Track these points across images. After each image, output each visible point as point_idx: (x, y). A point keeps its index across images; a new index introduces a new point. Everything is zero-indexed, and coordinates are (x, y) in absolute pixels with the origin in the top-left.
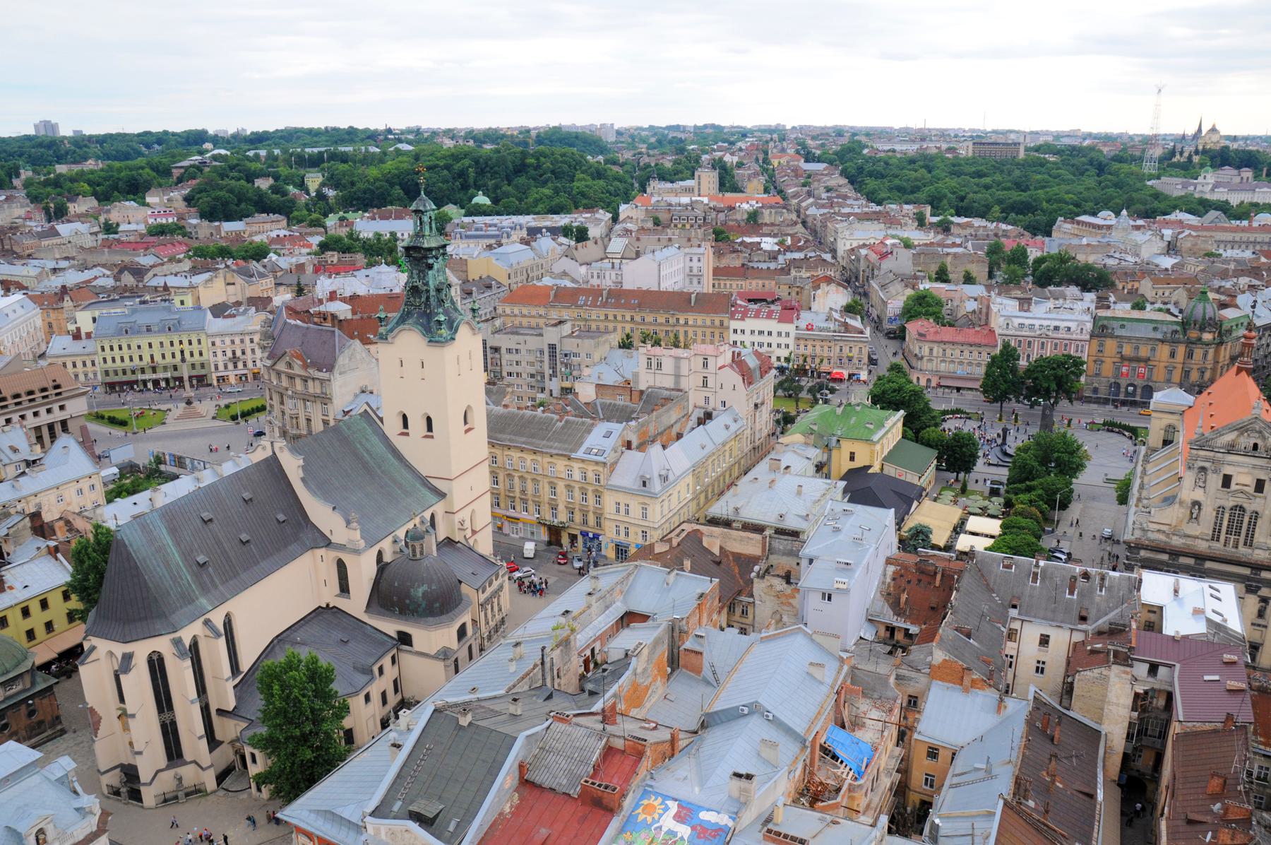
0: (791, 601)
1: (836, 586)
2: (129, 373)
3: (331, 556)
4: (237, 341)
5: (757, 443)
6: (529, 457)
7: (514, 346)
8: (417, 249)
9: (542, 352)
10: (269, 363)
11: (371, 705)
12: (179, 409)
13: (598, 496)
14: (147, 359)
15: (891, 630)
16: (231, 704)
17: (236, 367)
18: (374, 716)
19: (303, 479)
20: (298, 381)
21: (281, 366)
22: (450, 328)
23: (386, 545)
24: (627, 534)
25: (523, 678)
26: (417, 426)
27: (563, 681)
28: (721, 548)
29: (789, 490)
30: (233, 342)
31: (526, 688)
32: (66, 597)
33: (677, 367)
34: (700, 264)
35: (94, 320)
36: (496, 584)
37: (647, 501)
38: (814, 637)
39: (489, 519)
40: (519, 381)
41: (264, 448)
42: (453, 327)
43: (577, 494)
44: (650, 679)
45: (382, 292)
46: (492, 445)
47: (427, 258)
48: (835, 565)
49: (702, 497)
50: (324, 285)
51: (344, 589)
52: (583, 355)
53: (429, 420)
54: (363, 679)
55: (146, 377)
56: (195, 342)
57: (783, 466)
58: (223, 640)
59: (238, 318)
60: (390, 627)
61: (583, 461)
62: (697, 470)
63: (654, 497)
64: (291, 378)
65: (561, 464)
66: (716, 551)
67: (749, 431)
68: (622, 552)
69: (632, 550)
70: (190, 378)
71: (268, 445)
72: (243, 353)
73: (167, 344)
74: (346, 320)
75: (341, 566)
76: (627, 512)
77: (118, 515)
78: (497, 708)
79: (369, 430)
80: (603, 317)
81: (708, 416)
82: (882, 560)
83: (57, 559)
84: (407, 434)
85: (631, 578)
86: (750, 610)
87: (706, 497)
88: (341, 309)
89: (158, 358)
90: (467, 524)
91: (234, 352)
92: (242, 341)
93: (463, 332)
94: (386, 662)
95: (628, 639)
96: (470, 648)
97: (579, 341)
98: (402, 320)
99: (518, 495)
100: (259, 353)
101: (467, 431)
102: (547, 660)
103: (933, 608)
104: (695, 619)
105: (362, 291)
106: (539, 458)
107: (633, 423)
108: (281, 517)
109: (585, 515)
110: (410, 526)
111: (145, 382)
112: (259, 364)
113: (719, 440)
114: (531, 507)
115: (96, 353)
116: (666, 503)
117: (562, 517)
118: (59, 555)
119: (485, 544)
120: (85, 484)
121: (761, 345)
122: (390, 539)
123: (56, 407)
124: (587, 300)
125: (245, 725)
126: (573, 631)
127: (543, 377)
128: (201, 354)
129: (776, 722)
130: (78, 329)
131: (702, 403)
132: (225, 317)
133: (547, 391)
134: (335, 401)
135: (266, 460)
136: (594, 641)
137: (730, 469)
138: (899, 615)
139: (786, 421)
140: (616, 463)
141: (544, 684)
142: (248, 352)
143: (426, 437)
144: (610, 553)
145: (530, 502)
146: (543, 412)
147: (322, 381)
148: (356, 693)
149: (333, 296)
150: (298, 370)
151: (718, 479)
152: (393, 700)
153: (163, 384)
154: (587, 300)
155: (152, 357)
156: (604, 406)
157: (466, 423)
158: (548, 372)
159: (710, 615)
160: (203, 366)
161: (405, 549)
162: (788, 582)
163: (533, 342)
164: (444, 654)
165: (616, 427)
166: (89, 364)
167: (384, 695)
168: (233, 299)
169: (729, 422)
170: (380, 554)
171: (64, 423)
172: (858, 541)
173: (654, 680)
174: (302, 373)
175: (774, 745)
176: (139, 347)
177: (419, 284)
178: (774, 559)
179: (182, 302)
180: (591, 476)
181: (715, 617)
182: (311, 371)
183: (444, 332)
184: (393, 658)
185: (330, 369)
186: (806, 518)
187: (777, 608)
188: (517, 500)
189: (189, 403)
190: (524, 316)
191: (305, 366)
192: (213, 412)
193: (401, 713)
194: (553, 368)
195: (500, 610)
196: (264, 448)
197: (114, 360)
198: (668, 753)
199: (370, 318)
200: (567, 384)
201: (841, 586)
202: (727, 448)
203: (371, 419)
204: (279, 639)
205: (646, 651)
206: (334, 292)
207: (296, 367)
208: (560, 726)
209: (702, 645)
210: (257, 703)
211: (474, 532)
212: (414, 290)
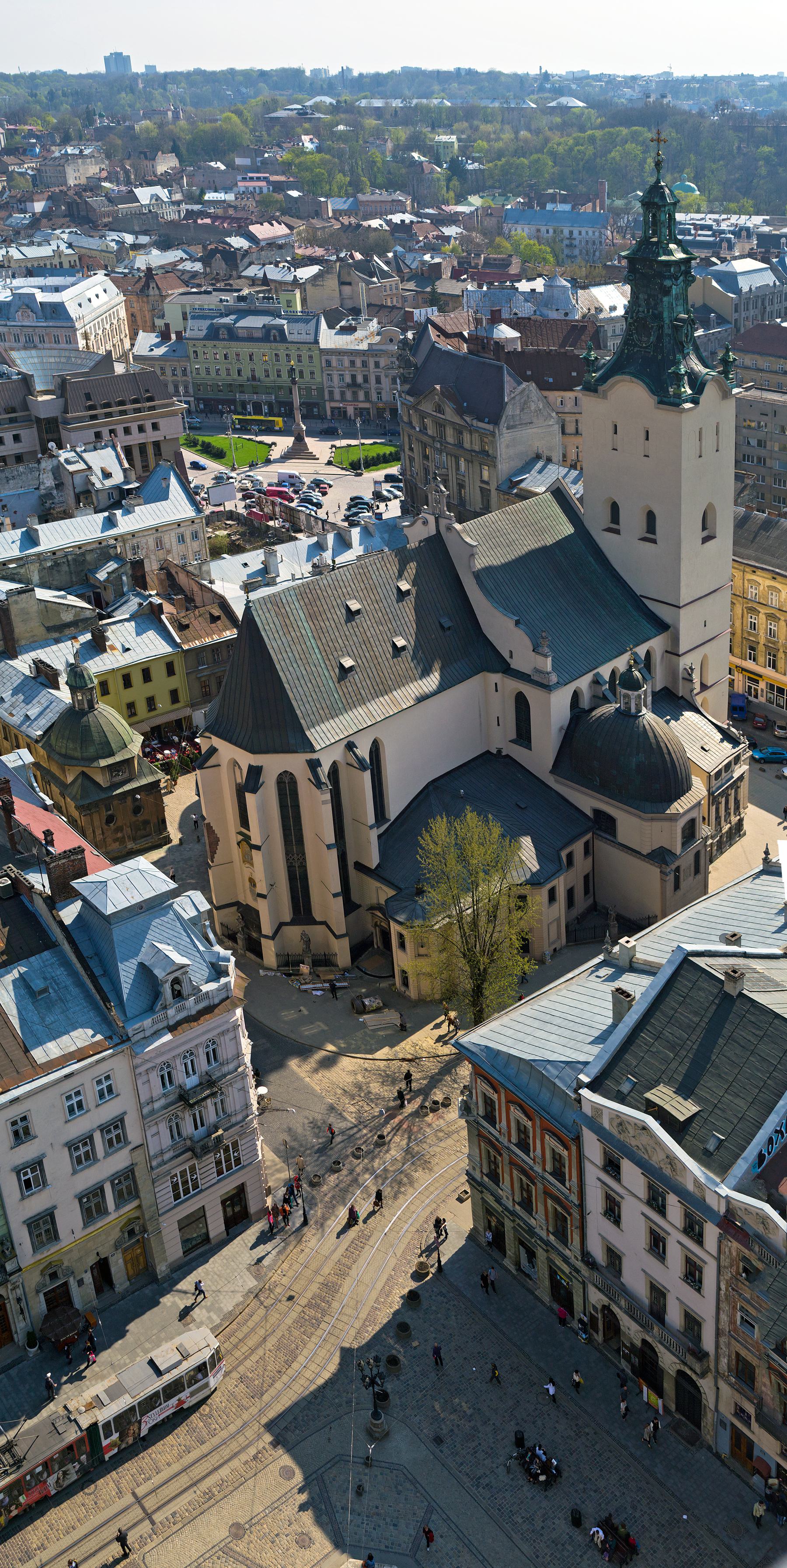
3: (516, 685)
4: (358, 363)
12: (285, 443)
14: (247, 373)
23: (584, 683)
30: (353, 363)
55: (246, 397)
56: (305, 359)
58: (367, 775)
60: (587, 802)
75: (522, 704)
91: (354, 377)
92: (365, 364)
100: (386, 383)
110: (621, 663)
112: (385, 397)
122: (589, 677)
147: (482, 435)
155: (253, 371)
168: (349, 304)
170: (576, 696)
171: (157, 445)
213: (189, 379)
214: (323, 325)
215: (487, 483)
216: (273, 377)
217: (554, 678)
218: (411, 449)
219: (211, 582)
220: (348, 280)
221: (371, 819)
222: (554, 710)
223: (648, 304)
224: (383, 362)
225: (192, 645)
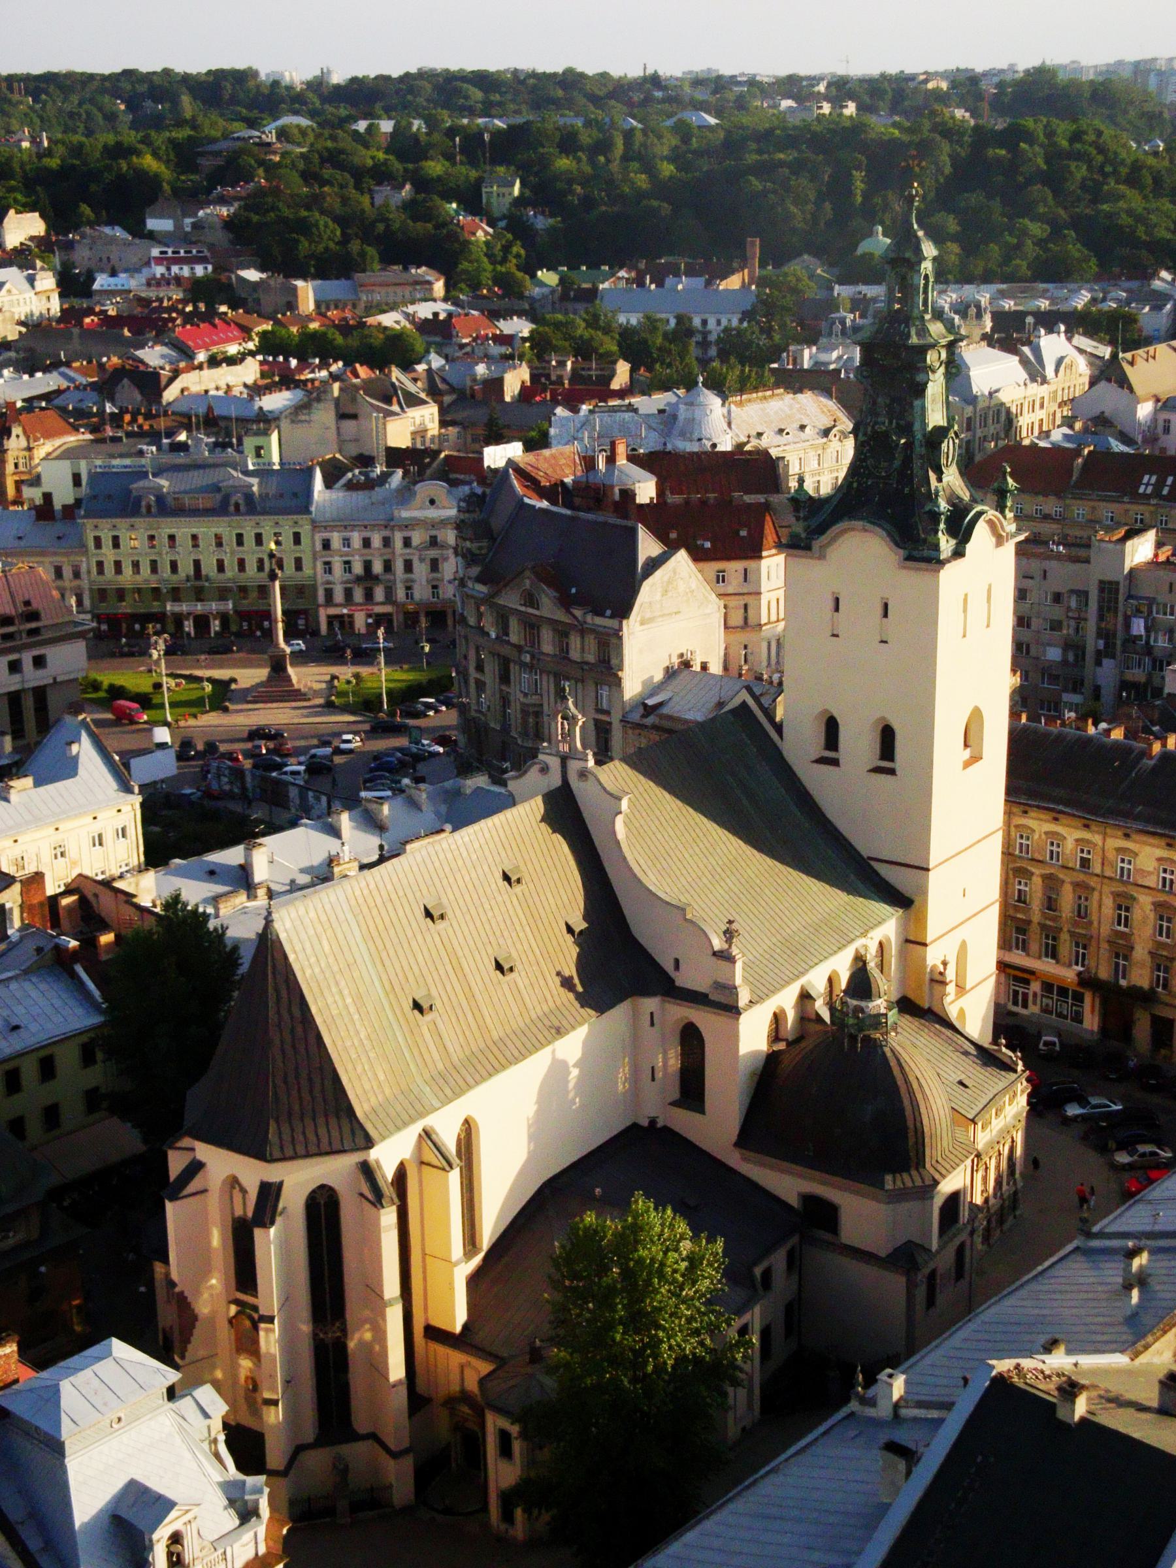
4: (377, 542)
9: (1083, 595)
14: (186, 569)
16: (458, 1317)
17: (369, 596)
21: (511, 600)
22: (952, 531)
26: (858, 745)
30: (367, 543)
32: (88, 1056)
39: (992, 967)
41: (545, 770)
51: (691, 1088)
53: (887, 736)
55: (184, 608)
71: (554, 763)
72: (388, 566)
73: (229, 537)
83: (73, 975)
84: (835, 762)
89: (209, 567)
90: (950, 975)
91: (368, 565)
92: (387, 542)
99: (1036, 917)
106: (1097, 839)
114: (1066, 947)
117: (1140, 977)
118: (79, 969)
123: (27, 658)
124: (1160, 484)
125: (485, 1367)
130: (47, 497)
142: (399, 566)
143: (877, 770)
145: (1065, 936)
150: (548, 607)
153: (216, 626)
154: (1160, 484)
155: (197, 564)
157: (966, 745)
158: (1093, 643)
167: (765, 1334)
168: (353, 450)
170: (778, 1018)
171: (40, 693)
174: (560, 616)
176: (172, 538)
182: (578, 613)
184: (791, 1256)
185: (624, 609)
188: (1034, 928)
189: (278, 667)
191: (566, 602)
196: (545, 770)
200: (1137, 675)
213: (85, 583)
215: (608, 713)
216: (231, 571)
218: (480, 668)
220: (352, 411)
224: (417, 538)
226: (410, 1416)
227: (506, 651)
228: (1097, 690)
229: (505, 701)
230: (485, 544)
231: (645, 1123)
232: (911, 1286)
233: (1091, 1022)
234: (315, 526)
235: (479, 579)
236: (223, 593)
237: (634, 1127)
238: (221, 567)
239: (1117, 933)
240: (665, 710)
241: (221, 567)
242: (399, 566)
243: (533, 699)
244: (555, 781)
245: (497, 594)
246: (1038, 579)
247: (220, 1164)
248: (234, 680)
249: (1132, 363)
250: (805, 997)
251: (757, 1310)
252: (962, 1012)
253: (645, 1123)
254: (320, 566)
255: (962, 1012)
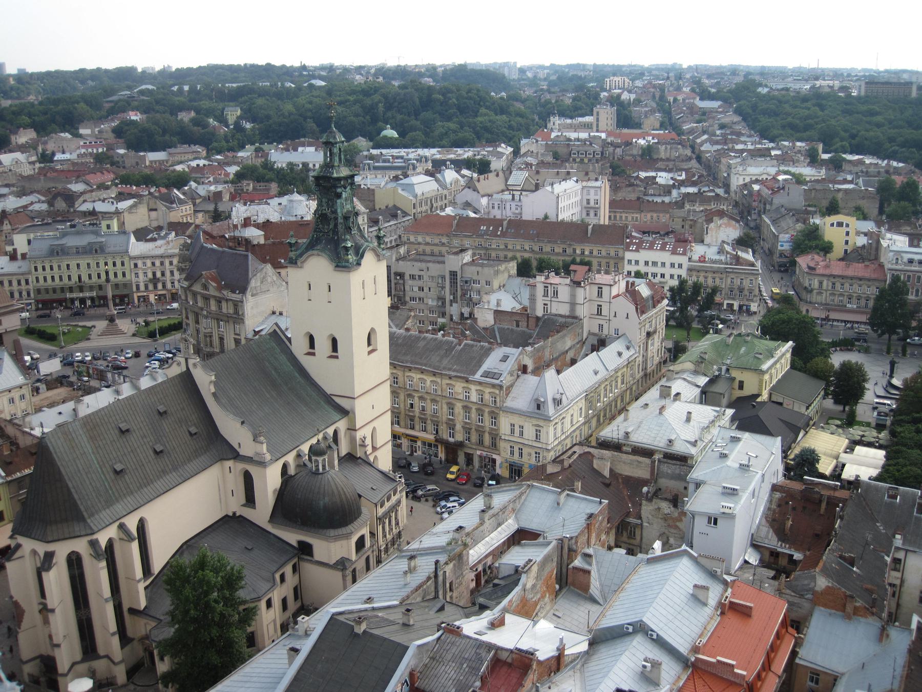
0: (678, 524)
1: (723, 510)
2: (58, 291)
3: (241, 466)
4: (158, 263)
5: (649, 370)
6: (429, 379)
7: (417, 273)
8: (328, 179)
9: (443, 277)
10: (186, 284)
11: (272, 611)
12: (101, 325)
13: (494, 416)
14: (75, 278)
15: (775, 554)
16: (143, 603)
17: (155, 287)
18: (274, 621)
19: (214, 394)
20: (213, 302)
21: (197, 288)
22: (357, 253)
24: (521, 455)
25: (417, 589)
27: (455, 595)
28: (611, 470)
29: (678, 417)
30: (153, 264)
31: (419, 599)
33: (573, 296)
34: (597, 197)
35: (29, 242)
36: (394, 499)
37: (541, 423)
38: (700, 559)
39: (389, 437)
40: (422, 306)
41: (179, 364)
42: (360, 254)
43: (474, 414)
44: (539, 596)
45: (294, 219)
46: (393, 365)
47: (336, 187)
48: (720, 490)
49: (594, 421)
50: (240, 211)
51: (250, 500)
52: (483, 282)
53: (334, 342)
54: (269, 585)
55: (74, 295)
56: (119, 264)
57: (673, 392)
59: (159, 243)
61: (480, 383)
62: (590, 397)
63: (547, 419)
64: (206, 298)
65: (459, 387)
66: (607, 473)
67: (641, 358)
68: (516, 472)
69: (526, 470)
70: (113, 296)
71: (183, 361)
72: (163, 274)
74: (258, 245)
76: (522, 433)
77: (45, 423)
78: (392, 617)
79: (278, 350)
80: (502, 247)
81: (601, 344)
82: (767, 488)
84: (313, 354)
85: (523, 497)
86: (638, 532)
87: (598, 420)
88: (254, 234)
89: (85, 278)
90: (368, 441)
91: (154, 274)
92: (162, 263)
93: (369, 259)
94: (288, 569)
95: (516, 557)
96: (368, 559)
97: (479, 269)
98: (311, 246)
99: (417, 414)
100: (177, 275)
101: (370, 353)
102: (440, 573)
103: (817, 535)
104: (584, 538)
105: (275, 217)
106: (439, 380)
107: (529, 349)
108: (193, 430)
109: (481, 432)
110: (314, 441)
111: (72, 300)
113: (612, 367)
115: (29, 273)
116: (559, 426)
117: (459, 437)
119: (385, 460)
120: (16, 395)
121: (654, 275)
122: (294, 453)
125: (154, 624)
126: (465, 545)
127: (444, 303)
128: (124, 275)
129: (660, 643)
130: (15, 250)
131: (596, 330)
132: (147, 241)
133: (447, 316)
134: (247, 322)
135: (181, 375)
136: (486, 556)
137: (622, 396)
138: (783, 541)
139: (676, 352)
140: (512, 386)
141: (436, 597)
142: (168, 274)
143: (331, 357)
144: (506, 474)
145: (429, 422)
146: (443, 336)
148: (259, 599)
149: (247, 222)
151: (610, 404)
152: (292, 606)
153: (89, 303)
155: (80, 277)
156: (501, 330)
157: (369, 344)
158: (448, 297)
159: (598, 536)
160: (125, 285)
161: (308, 464)
162: (675, 506)
163: (435, 269)
164: (342, 564)
165: (513, 352)
166: (23, 282)
167: (284, 601)
168: (155, 224)
169: (622, 348)
170: (285, 467)
172: (744, 468)
173: (543, 597)
174: (217, 294)
175: (656, 665)
176: (68, 266)
177: (328, 212)
178: (664, 482)
179: (108, 227)
180: (487, 397)
181: (603, 537)
182: (225, 293)
183: (351, 258)
184: (294, 567)
185: (243, 290)
186: (694, 444)
187: (663, 530)
188: (417, 419)
189: (112, 320)
190: (427, 244)
191: (220, 288)
192: (133, 328)
193: (299, 619)
194: (454, 294)
195: (397, 524)
196: (179, 364)
197: (45, 279)
198: (554, 667)
199: (282, 243)
201: (727, 511)
202: (619, 374)
203: (278, 338)
204: (187, 546)
205: (535, 568)
206: (249, 218)
207: (211, 288)
208: (451, 638)
209: (590, 564)
210: (166, 603)
211: (374, 449)
212: (321, 216)
214: (133, 239)
215: (239, 335)
216: (95, 278)
217: (268, 457)
219: (32, 429)
221: (139, 572)
222: (270, 481)
223: (328, 205)
225: (14, 477)
226: (122, 648)
227: (196, 310)
228: (451, 316)
229: (198, 331)
230: (187, 264)
231: (231, 514)
232: (344, 577)
233: (442, 455)
234: (131, 258)
235: (186, 279)
236: (91, 288)
237: (227, 516)
238: (90, 277)
239: (450, 419)
240: (263, 333)
241: (90, 277)
242: (168, 274)
243: (209, 330)
244: (184, 369)
245: (191, 285)
246: (425, 270)
247: (28, 545)
248: (94, 327)
249: (479, 181)
250: (299, 456)
251: (275, 592)
252: (376, 457)
253: (231, 514)
254: (133, 275)
255: (376, 457)
